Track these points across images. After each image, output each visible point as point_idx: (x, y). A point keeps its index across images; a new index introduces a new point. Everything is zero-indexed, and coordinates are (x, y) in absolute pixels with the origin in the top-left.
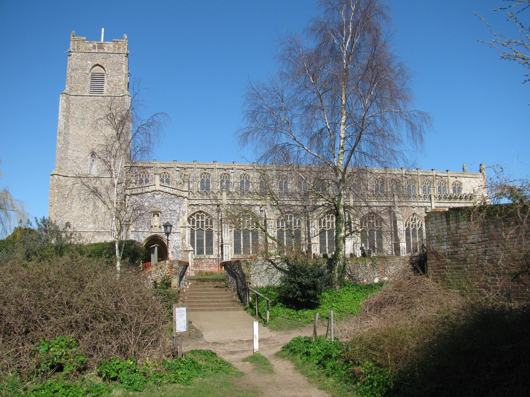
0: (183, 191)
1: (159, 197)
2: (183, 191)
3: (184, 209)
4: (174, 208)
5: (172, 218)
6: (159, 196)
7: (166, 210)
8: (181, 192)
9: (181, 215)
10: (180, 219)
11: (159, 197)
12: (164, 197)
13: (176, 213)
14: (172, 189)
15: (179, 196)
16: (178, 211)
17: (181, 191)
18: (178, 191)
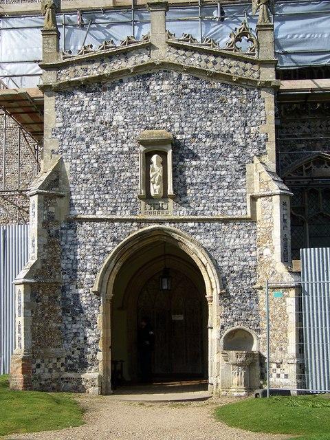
0: (254, 62)
1: (164, 87)
2: (254, 62)
3: (263, 128)
4: (225, 129)
5: (219, 163)
6: (166, 85)
7: (194, 136)
8: (248, 66)
9: (251, 151)
10: (249, 167)
11: (164, 87)
12: (185, 87)
13: (234, 143)
14: (212, 59)
15: (241, 79)
16: (238, 138)
17: (246, 61)
18: (233, 63)
